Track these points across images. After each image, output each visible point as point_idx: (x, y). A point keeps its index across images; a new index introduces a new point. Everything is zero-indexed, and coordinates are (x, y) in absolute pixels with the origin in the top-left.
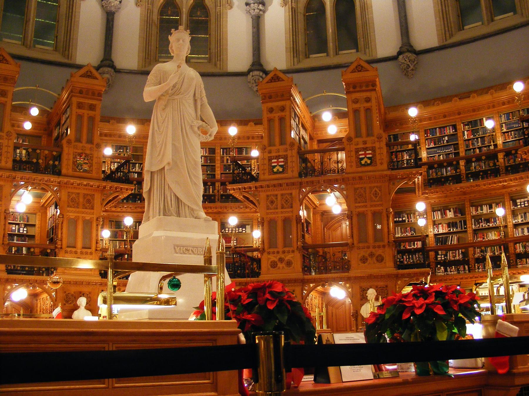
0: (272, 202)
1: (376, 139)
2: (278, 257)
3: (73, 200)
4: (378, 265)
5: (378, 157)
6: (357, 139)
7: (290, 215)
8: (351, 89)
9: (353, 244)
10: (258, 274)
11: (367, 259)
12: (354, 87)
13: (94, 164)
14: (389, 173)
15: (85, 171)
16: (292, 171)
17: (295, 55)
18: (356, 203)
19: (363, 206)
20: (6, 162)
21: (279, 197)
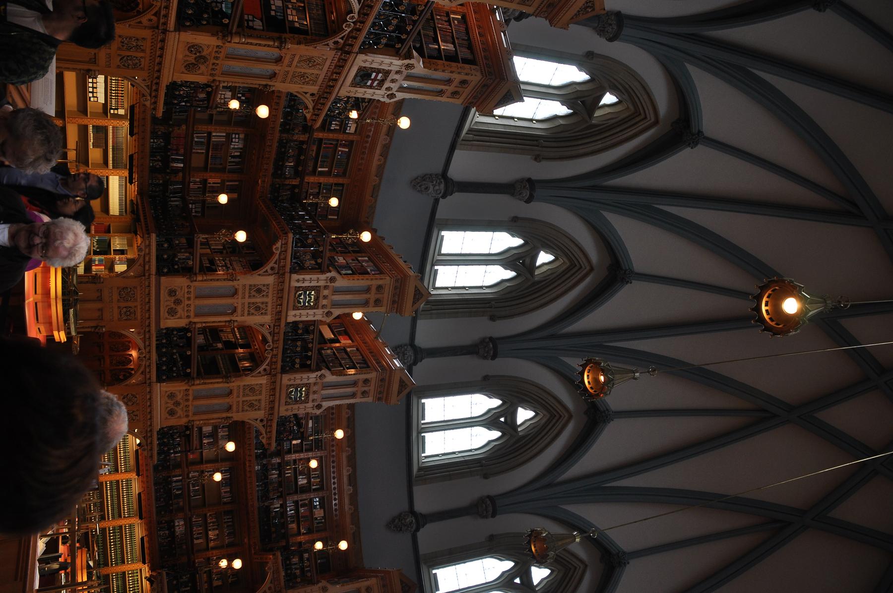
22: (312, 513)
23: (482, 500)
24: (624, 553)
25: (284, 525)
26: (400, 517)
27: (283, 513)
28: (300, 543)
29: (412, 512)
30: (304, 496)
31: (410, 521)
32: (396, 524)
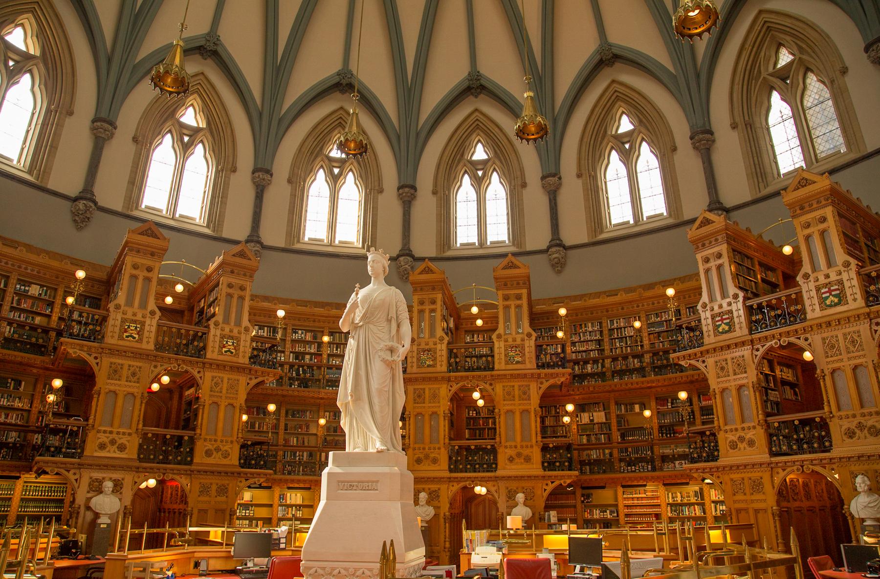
0: (722, 368)
1: (842, 269)
2: (738, 436)
3: (509, 394)
4: (871, 439)
5: (848, 292)
6: (815, 274)
7: (744, 381)
8: (798, 212)
9: (831, 413)
10: (715, 459)
11: (854, 433)
12: (802, 208)
13: (526, 354)
14: (867, 310)
15: (518, 362)
16: (741, 328)
17: (760, 179)
18: (827, 357)
19: (837, 361)
20: (441, 366)
21: (729, 361)
22: (32, 297)
23: (93, 129)
24: (208, 34)
25: (33, 328)
26: (74, 214)
27: (21, 325)
28: (60, 318)
29: (76, 200)
30: (8, 298)
31: (84, 205)
32: (81, 220)
